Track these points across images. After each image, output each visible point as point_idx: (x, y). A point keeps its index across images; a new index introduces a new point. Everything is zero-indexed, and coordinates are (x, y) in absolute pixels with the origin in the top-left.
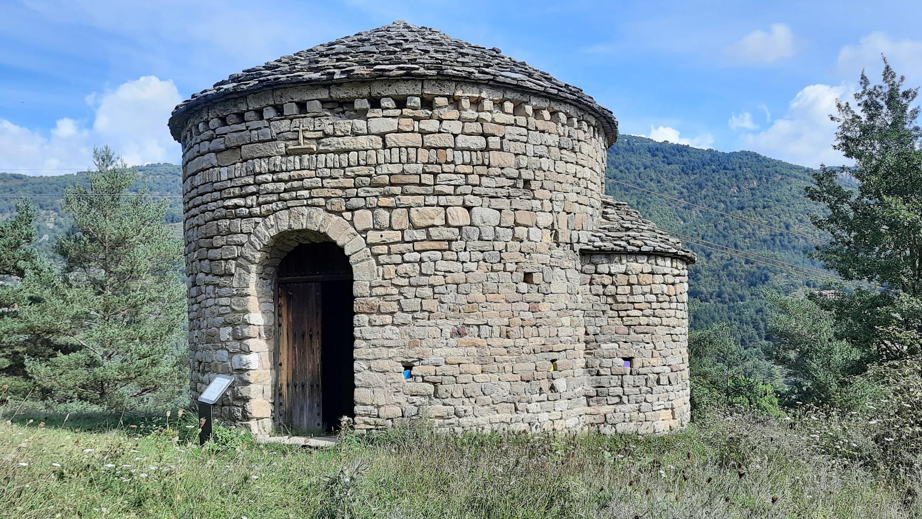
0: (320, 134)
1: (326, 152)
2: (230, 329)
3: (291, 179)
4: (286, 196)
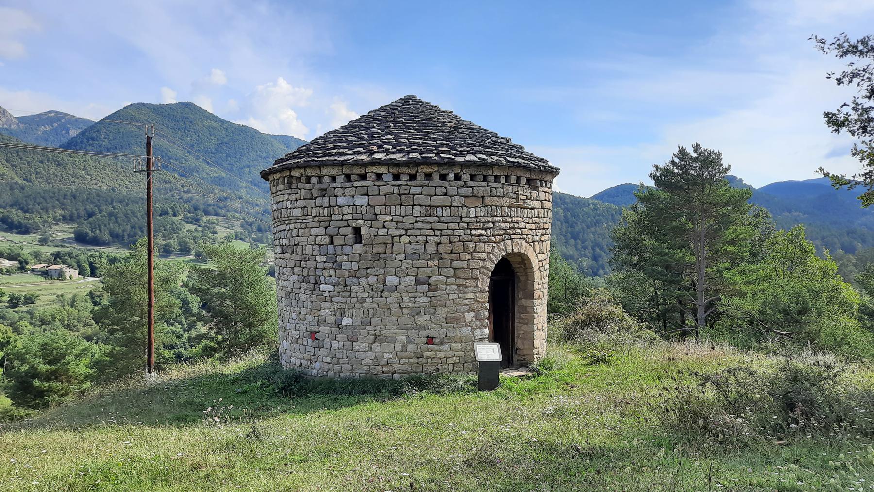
0: (525, 197)
1: (527, 208)
2: (473, 314)
3: (512, 222)
4: (511, 232)
